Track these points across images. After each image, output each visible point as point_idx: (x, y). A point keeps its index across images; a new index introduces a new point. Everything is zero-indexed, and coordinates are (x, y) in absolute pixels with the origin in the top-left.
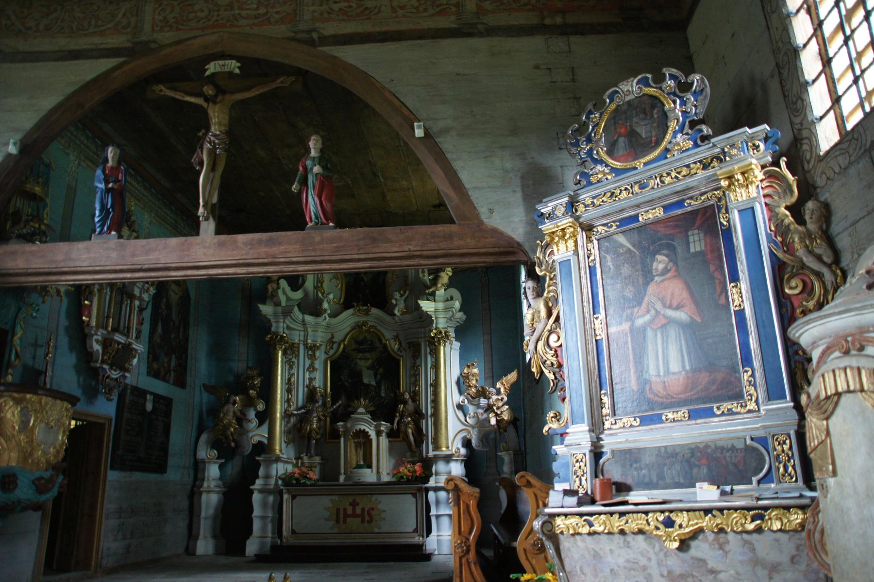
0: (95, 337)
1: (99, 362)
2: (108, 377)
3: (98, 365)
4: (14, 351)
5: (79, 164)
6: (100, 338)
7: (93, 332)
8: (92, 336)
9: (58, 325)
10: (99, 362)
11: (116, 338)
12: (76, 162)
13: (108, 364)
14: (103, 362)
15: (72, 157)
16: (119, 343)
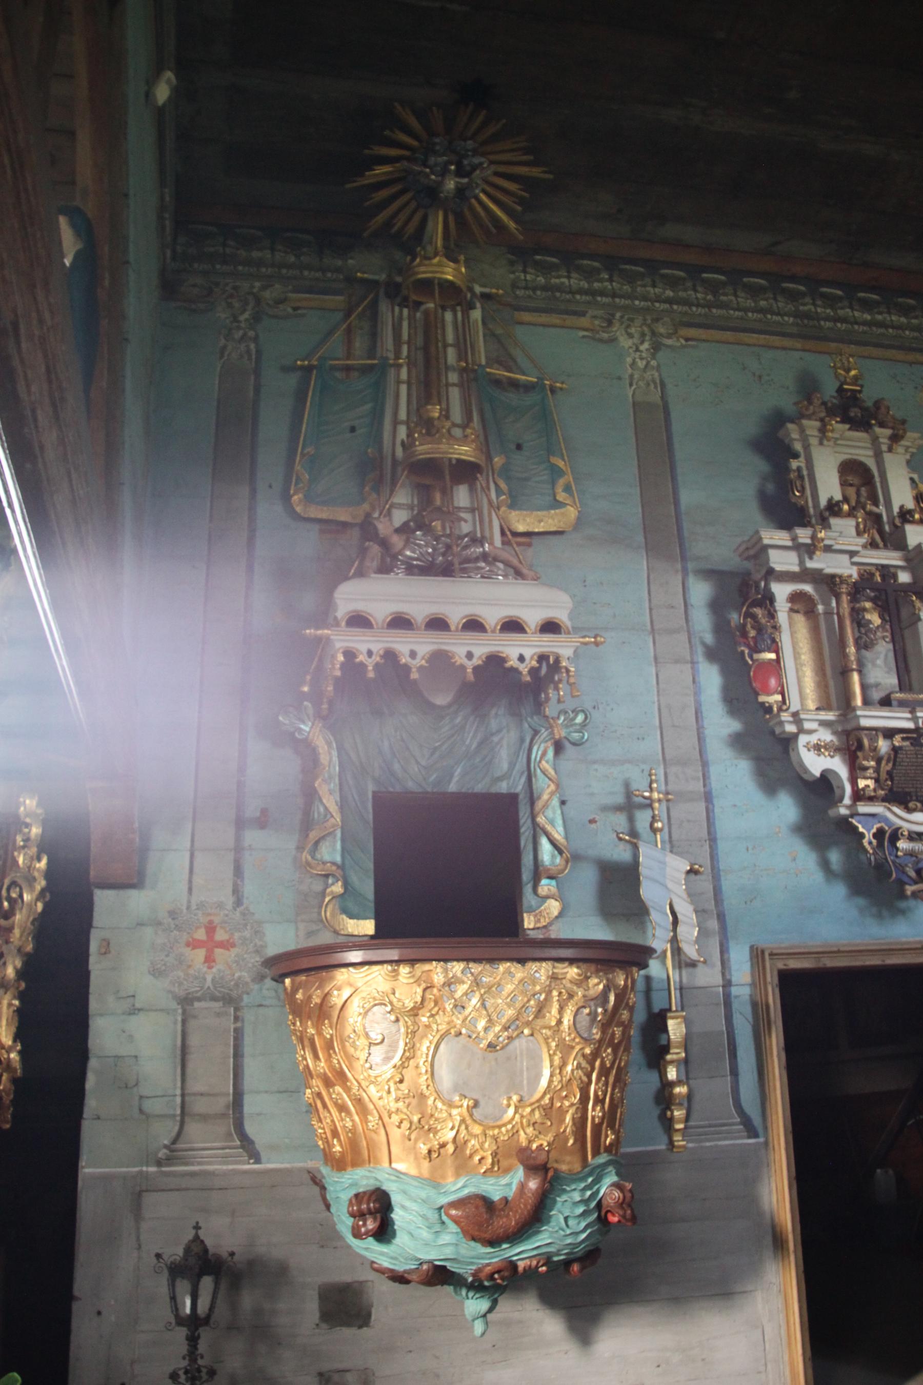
0: (803, 739)
1: (847, 801)
2: (895, 836)
3: (843, 811)
4: (544, 842)
5: (656, 348)
6: (826, 736)
7: (791, 728)
8: (794, 737)
9: (701, 739)
10: (847, 801)
11: (864, 722)
12: (645, 346)
13: (885, 799)
14: (858, 796)
15: (625, 343)
16: (889, 733)
